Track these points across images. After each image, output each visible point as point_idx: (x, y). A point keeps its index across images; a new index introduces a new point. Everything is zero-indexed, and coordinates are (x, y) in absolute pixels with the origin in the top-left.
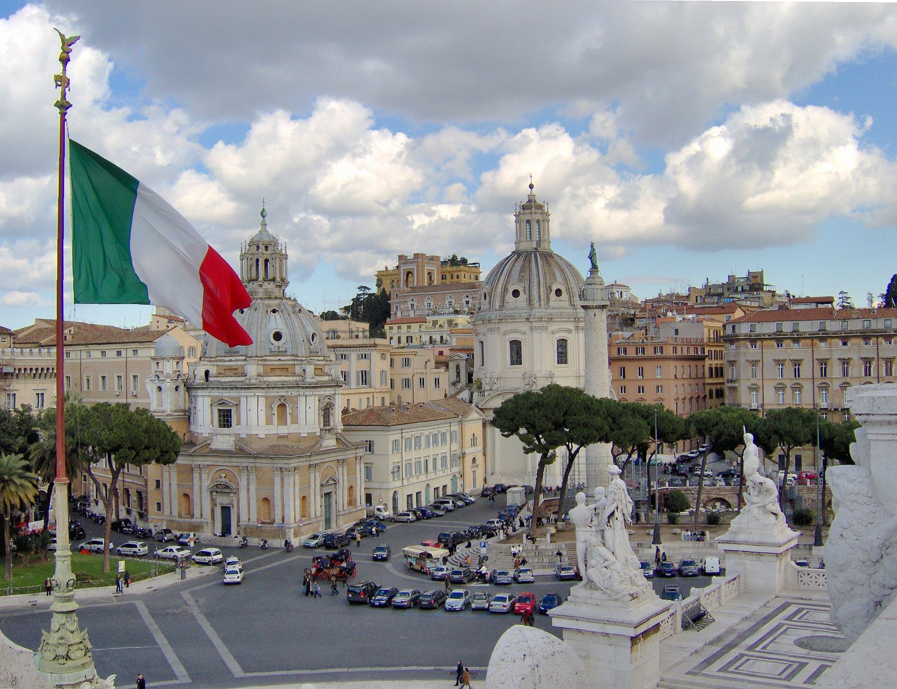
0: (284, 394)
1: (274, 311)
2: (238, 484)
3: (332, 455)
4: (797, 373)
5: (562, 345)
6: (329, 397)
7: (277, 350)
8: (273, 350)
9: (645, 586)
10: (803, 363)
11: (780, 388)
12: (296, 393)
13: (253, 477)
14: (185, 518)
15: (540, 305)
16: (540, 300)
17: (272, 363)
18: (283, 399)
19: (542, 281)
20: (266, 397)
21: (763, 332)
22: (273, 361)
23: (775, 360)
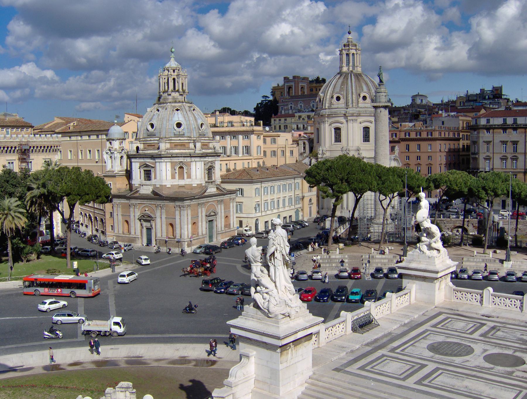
0: (182, 160)
1: (177, 110)
2: (155, 215)
3: (214, 198)
4: (515, 150)
5: (366, 130)
6: (212, 162)
7: (178, 134)
8: (176, 133)
9: (298, 308)
10: (519, 143)
11: (504, 159)
12: (190, 160)
13: (163, 211)
14: (126, 234)
15: (353, 106)
16: (352, 103)
17: (175, 141)
18: (182, 163)
19: (354, 91)
20: (171, 162)
21: (494, 124)
22: (177, 140)
23: (501, 141)
